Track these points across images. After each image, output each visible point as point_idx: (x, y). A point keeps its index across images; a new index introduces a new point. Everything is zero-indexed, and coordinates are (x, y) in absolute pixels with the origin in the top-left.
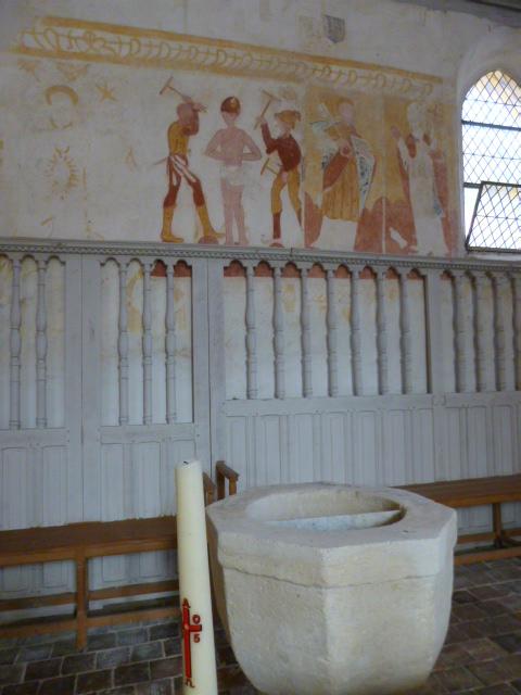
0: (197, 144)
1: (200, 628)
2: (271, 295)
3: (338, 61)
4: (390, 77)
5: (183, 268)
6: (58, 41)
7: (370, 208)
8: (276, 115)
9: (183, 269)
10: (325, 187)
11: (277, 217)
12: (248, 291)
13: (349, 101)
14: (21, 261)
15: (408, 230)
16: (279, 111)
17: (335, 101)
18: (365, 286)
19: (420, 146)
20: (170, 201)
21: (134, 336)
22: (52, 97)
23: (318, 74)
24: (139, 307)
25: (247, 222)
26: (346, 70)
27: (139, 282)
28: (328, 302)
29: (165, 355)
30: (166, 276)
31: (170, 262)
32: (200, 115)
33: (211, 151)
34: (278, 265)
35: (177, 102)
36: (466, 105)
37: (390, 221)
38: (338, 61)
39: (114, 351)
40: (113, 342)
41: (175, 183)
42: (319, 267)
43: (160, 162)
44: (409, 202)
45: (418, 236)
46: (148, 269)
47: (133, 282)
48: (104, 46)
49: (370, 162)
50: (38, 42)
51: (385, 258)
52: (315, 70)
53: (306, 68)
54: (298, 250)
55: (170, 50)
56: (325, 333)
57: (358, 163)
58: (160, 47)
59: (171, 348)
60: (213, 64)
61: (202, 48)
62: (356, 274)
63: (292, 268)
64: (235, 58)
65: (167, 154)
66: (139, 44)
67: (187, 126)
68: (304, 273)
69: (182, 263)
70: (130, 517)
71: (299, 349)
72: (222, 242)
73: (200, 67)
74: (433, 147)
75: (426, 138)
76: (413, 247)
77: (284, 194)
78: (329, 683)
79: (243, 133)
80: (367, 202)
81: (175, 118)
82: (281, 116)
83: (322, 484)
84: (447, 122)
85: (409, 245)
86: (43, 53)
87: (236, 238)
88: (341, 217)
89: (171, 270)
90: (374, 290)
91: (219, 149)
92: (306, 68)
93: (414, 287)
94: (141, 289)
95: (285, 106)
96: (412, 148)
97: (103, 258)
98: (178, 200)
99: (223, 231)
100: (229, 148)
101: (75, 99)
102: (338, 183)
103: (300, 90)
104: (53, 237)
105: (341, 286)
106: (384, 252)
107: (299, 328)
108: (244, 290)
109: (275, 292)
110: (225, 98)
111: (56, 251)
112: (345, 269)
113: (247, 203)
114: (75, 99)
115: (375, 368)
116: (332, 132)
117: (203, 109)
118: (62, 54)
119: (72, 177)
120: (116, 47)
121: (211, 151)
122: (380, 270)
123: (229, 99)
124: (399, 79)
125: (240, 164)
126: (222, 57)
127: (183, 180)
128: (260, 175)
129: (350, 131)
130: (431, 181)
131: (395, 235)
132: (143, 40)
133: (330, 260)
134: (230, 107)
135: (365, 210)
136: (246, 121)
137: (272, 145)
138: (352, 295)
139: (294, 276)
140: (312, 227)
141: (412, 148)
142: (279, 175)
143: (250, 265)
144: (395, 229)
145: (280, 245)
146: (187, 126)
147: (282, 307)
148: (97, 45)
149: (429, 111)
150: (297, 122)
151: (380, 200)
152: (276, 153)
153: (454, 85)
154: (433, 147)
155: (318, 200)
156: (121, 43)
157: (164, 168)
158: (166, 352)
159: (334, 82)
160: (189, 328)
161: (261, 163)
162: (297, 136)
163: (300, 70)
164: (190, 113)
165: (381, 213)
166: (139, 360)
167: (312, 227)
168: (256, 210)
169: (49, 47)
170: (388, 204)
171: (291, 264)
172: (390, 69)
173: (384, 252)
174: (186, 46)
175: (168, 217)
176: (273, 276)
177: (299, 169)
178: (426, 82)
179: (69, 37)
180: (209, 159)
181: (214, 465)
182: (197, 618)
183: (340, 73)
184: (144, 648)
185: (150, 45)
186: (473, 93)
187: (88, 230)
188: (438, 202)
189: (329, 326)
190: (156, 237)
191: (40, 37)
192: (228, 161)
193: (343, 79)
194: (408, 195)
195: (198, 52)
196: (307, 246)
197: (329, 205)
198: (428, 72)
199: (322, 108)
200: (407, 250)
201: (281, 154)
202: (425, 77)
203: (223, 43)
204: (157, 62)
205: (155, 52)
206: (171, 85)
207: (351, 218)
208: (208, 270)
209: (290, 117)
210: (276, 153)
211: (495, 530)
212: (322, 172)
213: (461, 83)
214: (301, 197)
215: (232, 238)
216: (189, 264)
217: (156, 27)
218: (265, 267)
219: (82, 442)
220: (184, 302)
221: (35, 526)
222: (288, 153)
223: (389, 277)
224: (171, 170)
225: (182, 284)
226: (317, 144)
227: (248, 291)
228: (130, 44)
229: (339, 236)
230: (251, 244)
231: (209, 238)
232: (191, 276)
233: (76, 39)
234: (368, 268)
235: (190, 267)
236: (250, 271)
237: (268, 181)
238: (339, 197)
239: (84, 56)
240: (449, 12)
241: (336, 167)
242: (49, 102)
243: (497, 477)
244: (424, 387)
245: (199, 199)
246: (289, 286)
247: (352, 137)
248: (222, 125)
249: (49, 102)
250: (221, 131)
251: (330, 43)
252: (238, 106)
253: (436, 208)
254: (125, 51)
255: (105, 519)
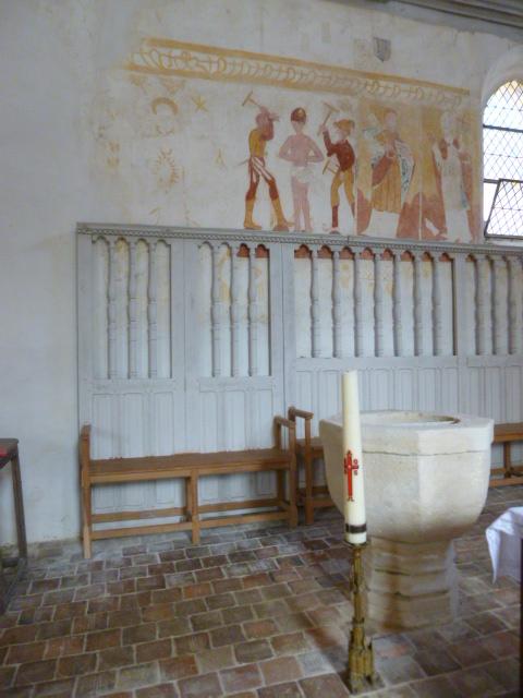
0: (272, 148)
1: (357, 467)
2: (331, 274)
3: (385, 77)
4: (427, 91)
5: (263, 251)
6: (160, 61)
7: (410, 202)
8: (335, 123)
9: (262, 252)
10: (374, 184)
11: (335, 209)
12: (313, 270)
13: (394, 112)
14: (136, 243)
15: (440, 221)
16: (338, 120)
17: (383, 112)
18: (405, 267)
19: (451, 149)
20: (251, 195)
21: (223, 306)
22: (158, 108)
23: (369, 88)
24: (228, 283)
25: (312, 213)
26: (391, 85)
27: (227, 263)
28: (375, 280)
29: (247, 321)
30: (248, 256)
31: (253, 246)
32: (275, 123)
33: (283, 154)
34: (337, 249)
35: (256, 112)
36: (487, 111)
37: (426, 213)
38: (385, 77)
39: (208, 317)
40: (208, 310)
41: (255, 181)
42: (369, 252)
43: (243, 163)
44: (441, 197)
45: (449, 225)
46: (236, 251)
47: (222, 261)
48: (197, 65)
49: (410, 164)
50: (144, 60)
51: (420, 246)
52: (366, 84)
53: (359, 83)
54: (353, 238)
55: (250, 67)
56: (373, 305)
57: (400, 164)
58: (242, 65)
59: (253, 315)
60: (285, 81)
61: (275, 66)
62: (398, 258)
63: (348, 251)
64: (302, 75)
65: (248, 157)
66: (225, 62)
67: (264, 133)
68: (357, 255)
69: (261, 246)
70: (222, 450)
71: (352, 317)
72: (292, 229)
73: (274, 82)
74: (460, 150)
75: (456, 143)
76: (444, 235)
77: (341, 190)
78: (419, 515)
79: (309, 140)
80: (407, 197)
81: (254, 126)
82: (339, 125)
83: (393, 410)
84: (471, 126)
85: (441, 233)
86: (148, 70)
87: (303, 227)
88: (387, 209)
89: (253, 252)
90: (412, 270)
91: (289, 152)
92: (359, 83)
93: (444, 268)
94: (229, 268)
95: (343, 116)
96: (444, 151)
97: (200, 242)
98: (257, 195)
99: (293, 221)
100: (298, 151)
101: (175, 109)
102: (385, 181)
103: (354, 102)
104: (160, 224)
105: (386, 266)
106: (420, 239)
107: (352, 301)
108: (310, 269)
109: (334, 271)
110: (294, 109)
111: (165, 236)
112: (389, 253)
113: (311, 197)
114: (175, 109)
115: (412, 334)
116: (380, 138)
117: (277, 118)
118: (167, 72)
119: (174, 174)
120: (206, 65)
121: (283, 154)
122: (418, 254)
123: (297, 110)
124: (435, 92)
125: (306, 165)
126: (291, 75)
127: (261, 178)
128: (322, 174)
129: (393, 137)
130: (459, 179)
131: (430, 225)
132: (229, 60)
133: (378, 245)
134: (298, 117)
135: (405, 204)
136: (311, 129)
137: (333, 149)
138: (395, 274)
139: (327, 257)
140: (363, 219)
141: (444, 151)
142: (337, 175)
143: (315, 248)
144: (429, 219)
145: (338, 233)
146: (264, 133)
147: (339, 284)
148: (192, 63)
149: (458, 119)
150: (352, 130)
151: (418, 196)
152: (334, 157)
153: (479, 97)
154: (460, 150)
155: (368, 196)
156: (210, 62)
157: (246, 168)
158: (249, 318)
159: (381, 95)
160: (266, 299)
161: (323, 164)
162: (352, 142)
163: (355, 85)
164: (267, 121)
165: (418, 207)
166: (228, 325)
167: (363, 219)
168: (319, 205)
169: (154, 66)
170: (424, 198)
171: (347, 249)
172: (428, 84)
173: (420, 239)
174: (262, 64)
175: (249, 209)
176: (332, 258)
177: (353, 170)
178: (456, 94)
179: (170, 57)
180: (283, 161)
181: (287, 410)
182: (356, 461)
183: (386, 88)
184: (246, 543)
185: (234, 64)
186: (495, 100)
187: (187, 219)
188: (465, 198)
189: (376, 300)
190: (240, 225)
191: (146, 57)
192: (297, 163)
193: (389, 93)
194: (440, 192)
195: (272, 70)
196: (359, 233)
197: (377, 198)
198: (458, 84)
199: (372, 118)
200: (438, 237)
201: (339, 157)
202: (455, 90)
203: (292, 62)
204: (239, 78)
205: (238, 69)
206: (252, 97)
207: (394, 211)
208: (282, 253)
209: (346, 126)
210: (334, 157)
211: (505, 466)
212: (371, 172)
213: (484, 93)
214: (355, 193)
215: (299, 227)
216: (267, 247)
217: (238, 48)
218: (327, 251)
219: (185, 389)
220: (263, 278)
221: (149, 455)
222: (344, 156)
223: (423, 260)
224: (252, 170)
225: (261, 264)
226: (369, 149)
227: (313, 270)
228: (218, 62)
229: (384, 225)
230: (315, 232)
231: (281, 226)
232: (268, 257)
233: (175, 58)
234: (408, 252)
235: (268, 251)
236: (315, 254)
237: (329, 179)
238: (385, 192)
239: (179, 72)
240: (476, 34)
241: (383, 168)
242: (155, 112)
243: (508, 424)
244: (451, 350)
245: (274, 194)
246: (345, 265)
247: (396, 142)
248: (292, 132)
249: (155, 112)
250: (291, 137)
251: (379, 61)
252: (305, 115)
253: (464, 202)
254: (214, 69)
255: (202, 451)
